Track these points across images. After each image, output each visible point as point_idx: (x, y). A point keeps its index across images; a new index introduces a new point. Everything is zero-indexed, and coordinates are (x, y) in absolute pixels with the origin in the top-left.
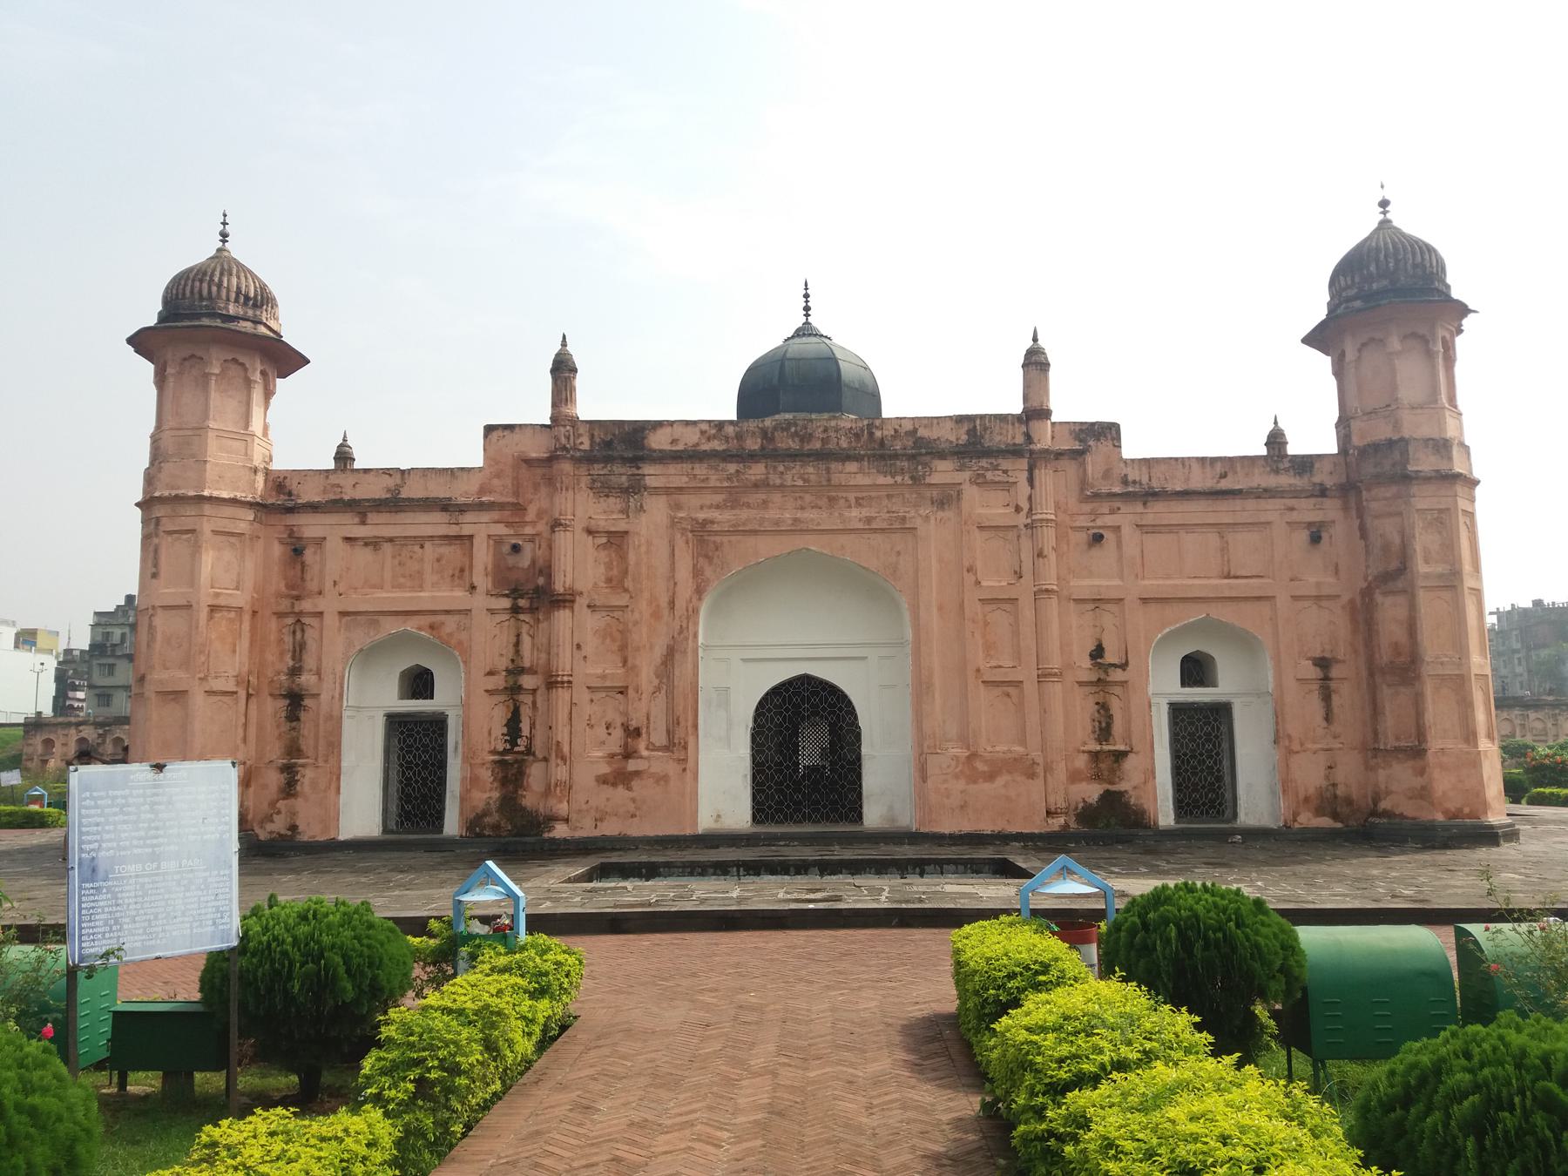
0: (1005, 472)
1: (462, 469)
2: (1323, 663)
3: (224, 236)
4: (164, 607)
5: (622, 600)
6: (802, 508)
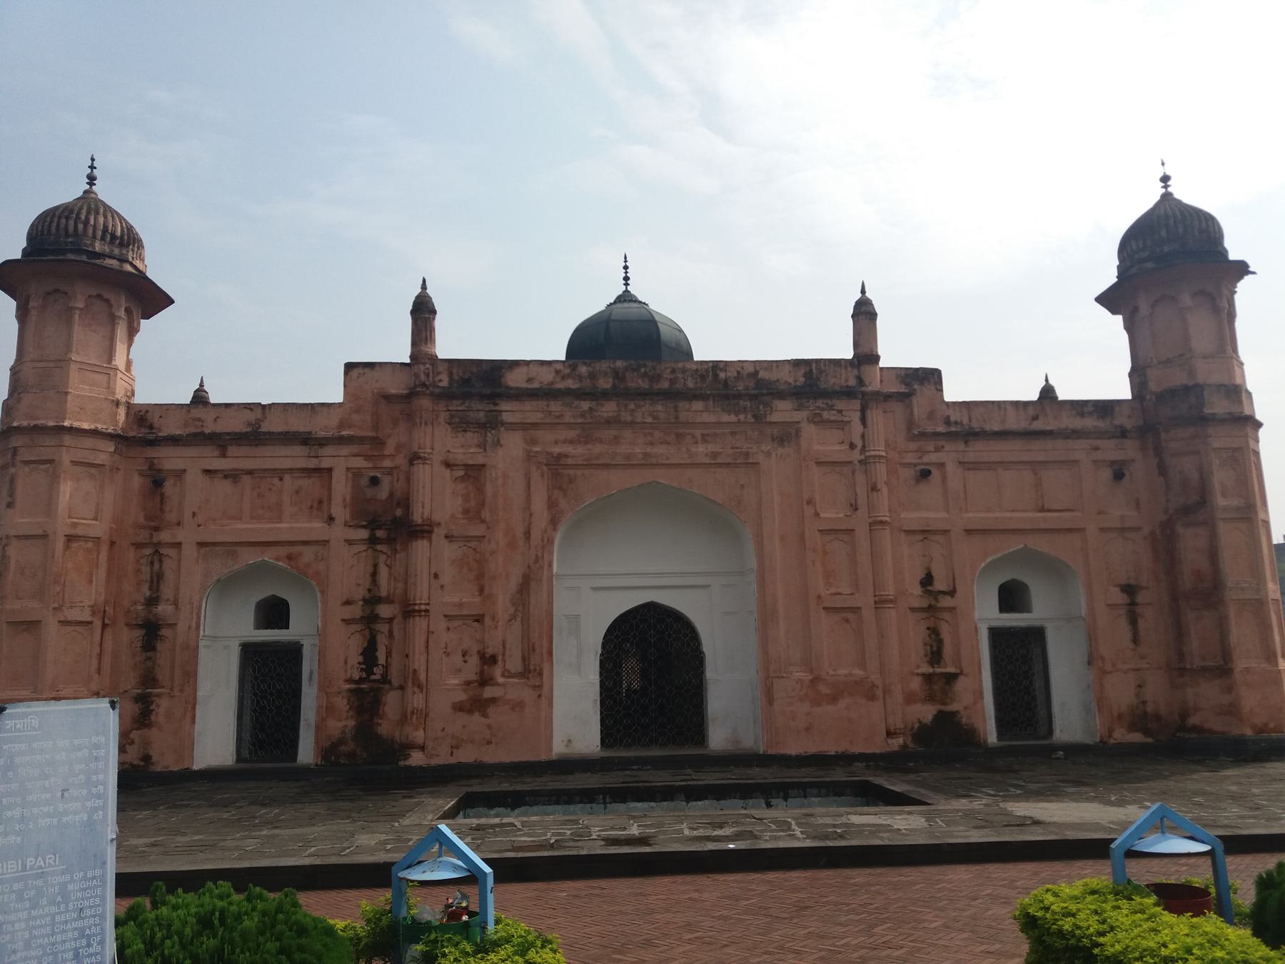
0: (840, 412)
1: (323, 404)
3: (92, 179)
4: (18, 537)
5: (477, 530)
6: (652, 444)
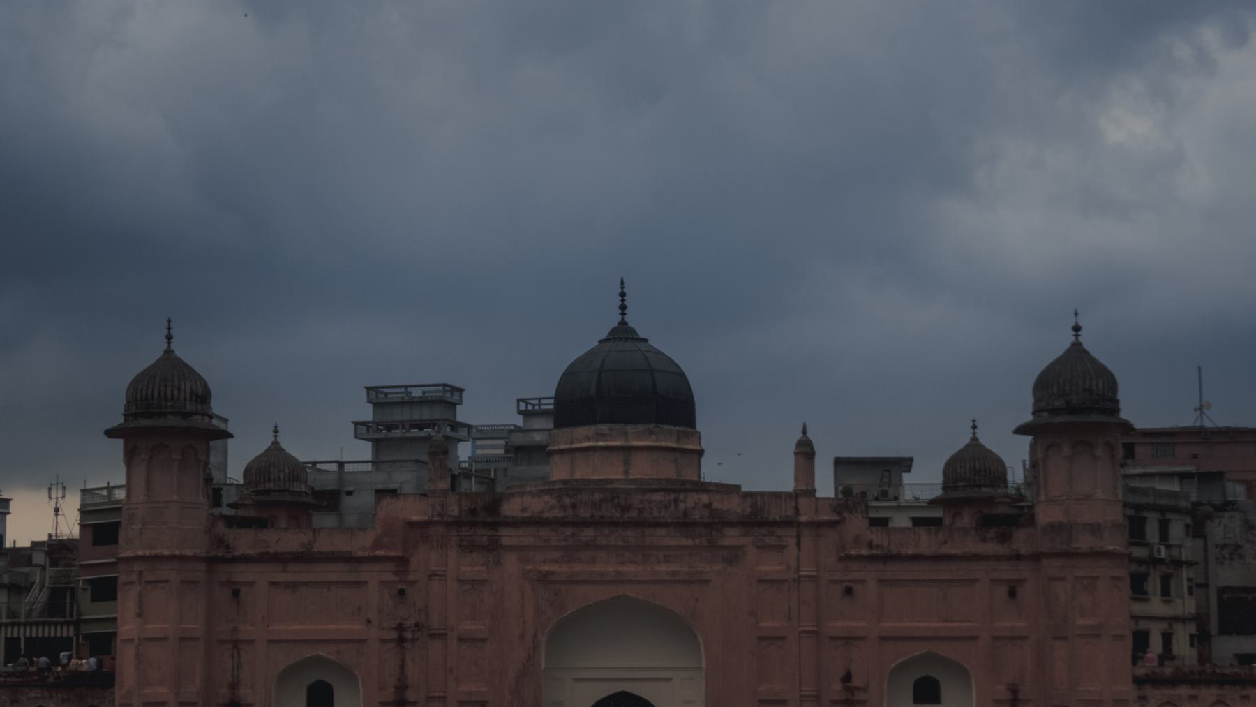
0: (779, 537)
3: (169, 337)
6: (622, 563)
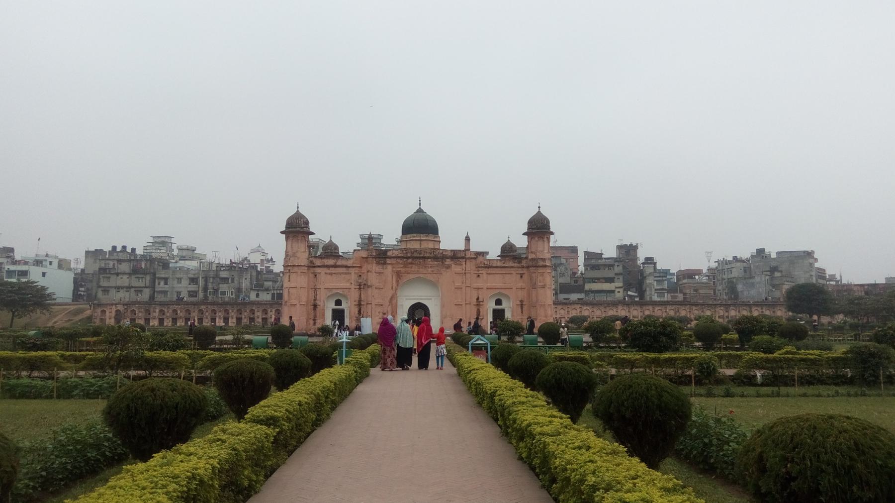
2: (521, 301)
